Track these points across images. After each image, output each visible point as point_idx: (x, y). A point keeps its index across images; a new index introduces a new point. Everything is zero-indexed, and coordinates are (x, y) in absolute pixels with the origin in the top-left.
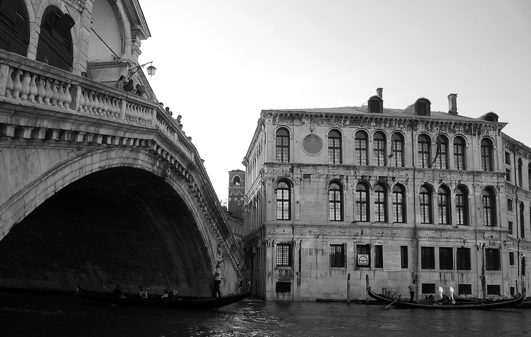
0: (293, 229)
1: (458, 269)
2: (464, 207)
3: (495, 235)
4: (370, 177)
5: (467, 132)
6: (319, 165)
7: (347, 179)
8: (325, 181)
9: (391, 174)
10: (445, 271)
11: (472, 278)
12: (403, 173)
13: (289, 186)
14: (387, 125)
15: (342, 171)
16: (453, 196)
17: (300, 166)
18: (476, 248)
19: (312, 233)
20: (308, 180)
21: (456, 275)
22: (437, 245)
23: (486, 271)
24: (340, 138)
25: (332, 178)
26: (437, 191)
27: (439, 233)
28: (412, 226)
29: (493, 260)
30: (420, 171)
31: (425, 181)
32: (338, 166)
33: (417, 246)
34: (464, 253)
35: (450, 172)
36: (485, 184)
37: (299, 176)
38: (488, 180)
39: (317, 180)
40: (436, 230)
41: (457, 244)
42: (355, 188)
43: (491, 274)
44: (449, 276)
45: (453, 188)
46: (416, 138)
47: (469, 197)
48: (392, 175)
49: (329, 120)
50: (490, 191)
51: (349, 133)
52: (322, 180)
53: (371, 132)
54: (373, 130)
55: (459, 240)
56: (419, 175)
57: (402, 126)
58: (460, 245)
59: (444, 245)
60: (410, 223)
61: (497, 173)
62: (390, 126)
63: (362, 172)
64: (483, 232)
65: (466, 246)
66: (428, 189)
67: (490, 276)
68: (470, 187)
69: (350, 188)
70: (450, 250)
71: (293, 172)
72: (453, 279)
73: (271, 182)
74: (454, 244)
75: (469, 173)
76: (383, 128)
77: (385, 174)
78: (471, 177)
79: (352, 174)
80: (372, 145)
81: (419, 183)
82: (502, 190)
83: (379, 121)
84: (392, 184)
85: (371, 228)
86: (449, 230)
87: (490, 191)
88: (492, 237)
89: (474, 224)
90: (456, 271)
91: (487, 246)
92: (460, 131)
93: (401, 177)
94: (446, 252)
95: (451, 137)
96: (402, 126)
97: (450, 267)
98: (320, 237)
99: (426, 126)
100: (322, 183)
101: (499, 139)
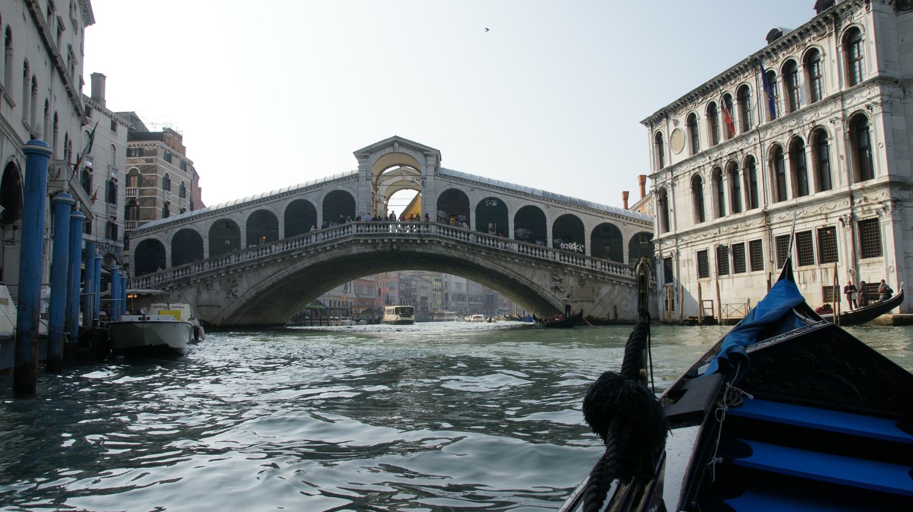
10: (804, 268)
18: (841, 223)
21: (818, 272)
23: (861, 261)
31: (774, 140)
33: (770, 235)
34: (827, 236)
43: (868, 264)
44: (810, 274)
55: (819, 217)
58: (820, 224)
59: (800, 228)
67: (866, 267)
81: (768, 144)
84: (740, 159)
88: (865, 199)
91: (860, 215)
94: (803, 238)
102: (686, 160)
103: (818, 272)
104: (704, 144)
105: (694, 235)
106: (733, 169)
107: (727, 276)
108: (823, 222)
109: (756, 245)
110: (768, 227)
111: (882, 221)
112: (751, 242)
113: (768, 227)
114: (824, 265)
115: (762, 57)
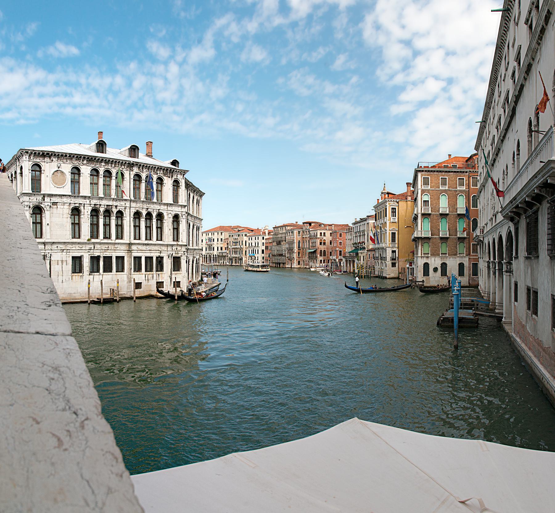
0: (45, 246)
1: (156, 271)
2: (160, 228)
3: (179, 248)
4: (100, 205)
5: (165, 175)
6: (64, 195)
7: (84, 206)
8: (68, 207)
9: (115, 203)
10: (148, 273)
11: (165, 276)
12: (123, 203)
13: (41, 211)
14: (113, 166)
15: (81, 201)
16: (154, 221)
17: (51, 196)
19: (59, 248)
20: (56, 206)
21: (155, 275)
22: (143, 256)
23: (173, 272)
24: (79, 175)
25: (72, 206)
26: (144, 217)
27: (145, 247)
28: (128, 242)
29: (176, 263)
30: (134, 201)
31: (137, 209)
32: (78, 196)
34: (160, 260)
35: (154, 203)
36: (173, 213)
37: (49, 204)
38: (176, 210)
39: (62, 207)
40: (144, 244)
41: (156, 254)
42: (89, 213)
44: (151, 276)
45: (154, 215)
46: (132, 177)
47: (164, 221)
48: (115, 205)
49: (71, 159)
50: (176, 218)
51: (86, 170)
52: (66, 207)
53: (102, 171)
54: (103, 169)
56: (133, 205)
57: (123, 167)
58: (158, 255)
59: (148, 255)
60: (126, 240)
61: (181, 206)
62: (115, 167)
63: (94, 202)
64: (172, 245)
65: (162, 255)
66: (137, 215)
68: (165, 214)
69: (86, 213)
70: (151, 258)
71: (44, 200)
72: (153, 277)
73: (28, 208)
74: (155, 255)
75: (165, 204)
76: (110, 167)
77: (110, 203)
78: (166, 207)
79: (88, 202)
80: (101, 181)
81: (133, 210)
82: (184, 217)
83: (107, 161)
84: (115, 211)
85: (100, 243)
86: (151, 244)
87: (176, 218)
89: (167, 240)
90: (155, 273)
92: (160, 173)
93: (121, 205)
94: (149, 259)
95: (155, 177)
96: (123, 167)
97: (151, 270)
98: (65, 251)
99: (139, 168)
100: (66, 210)
101: (183, 181)
102: (69, 196)
103: (155, 275)
104: (85, 189)
105: (71, 246)
106: (108, 213)
107: (98, 274)
108: (159, 254)
109: (120, 259)
110: (130, 251)
111: (182, 258)
112: (116, 257)
113: (130, 251)
114: (158, 273)
115: (137, 165)
